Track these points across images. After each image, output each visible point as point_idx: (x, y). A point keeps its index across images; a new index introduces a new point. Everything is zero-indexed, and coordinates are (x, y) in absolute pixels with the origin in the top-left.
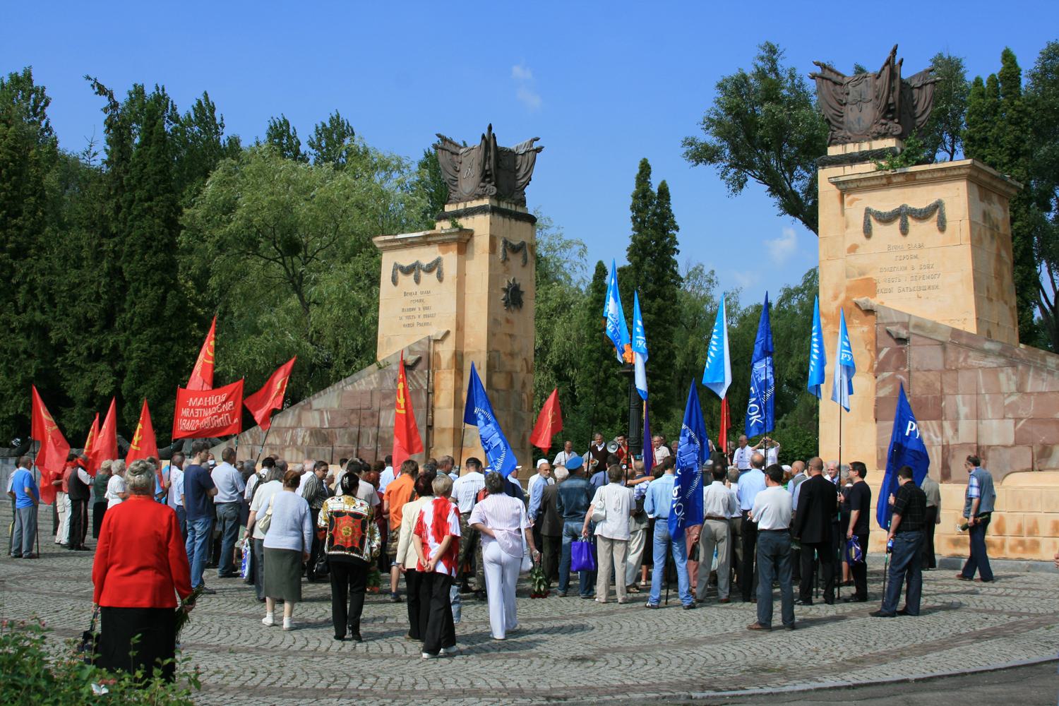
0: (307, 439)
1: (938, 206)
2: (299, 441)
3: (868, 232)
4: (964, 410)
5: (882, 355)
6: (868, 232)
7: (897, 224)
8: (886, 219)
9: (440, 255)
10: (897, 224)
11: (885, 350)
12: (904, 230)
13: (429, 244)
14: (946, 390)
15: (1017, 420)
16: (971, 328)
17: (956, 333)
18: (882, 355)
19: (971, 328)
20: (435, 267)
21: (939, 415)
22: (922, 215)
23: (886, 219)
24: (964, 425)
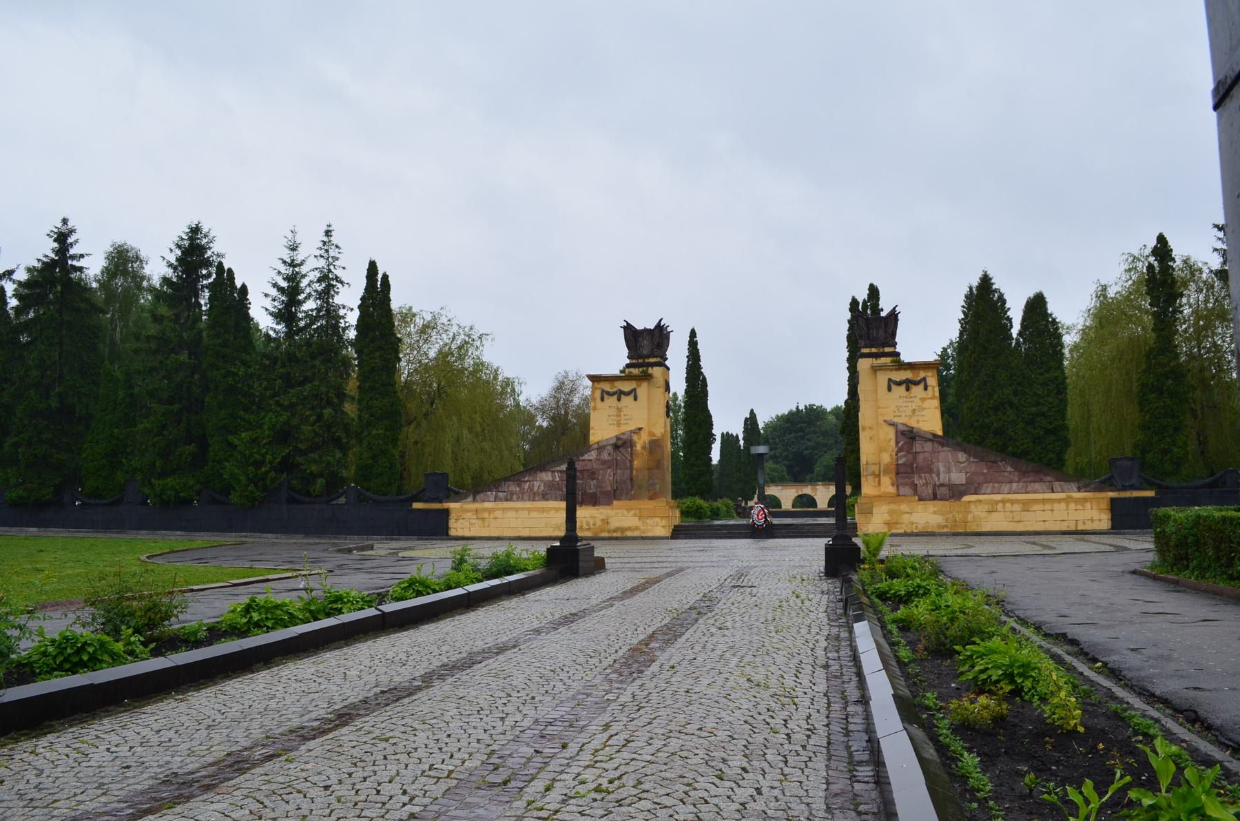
0: (542, 488)
1: (924, 379)
2: (536, 489)
3: (890, 389)
4: (942, 469)
5: (900, 445)
6: (890, 389)
7: (904, 387)
8: (899, 384)
9: (635, 386)
10: (904, 387)
11: (902, 443)
12: (908, 389)
13: (631, 380)
14: (934, 461)
15: (967, 473)
16: (940, 433)
17: (935, 436)
18: (900, 445)
19: (940, 433)
20: (633, 392)
21: (930, 471)
22: (917, 383)
23: (899, 384)
24: (942, 476)
